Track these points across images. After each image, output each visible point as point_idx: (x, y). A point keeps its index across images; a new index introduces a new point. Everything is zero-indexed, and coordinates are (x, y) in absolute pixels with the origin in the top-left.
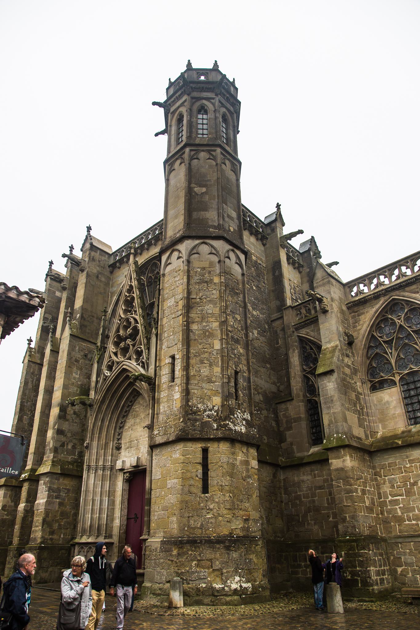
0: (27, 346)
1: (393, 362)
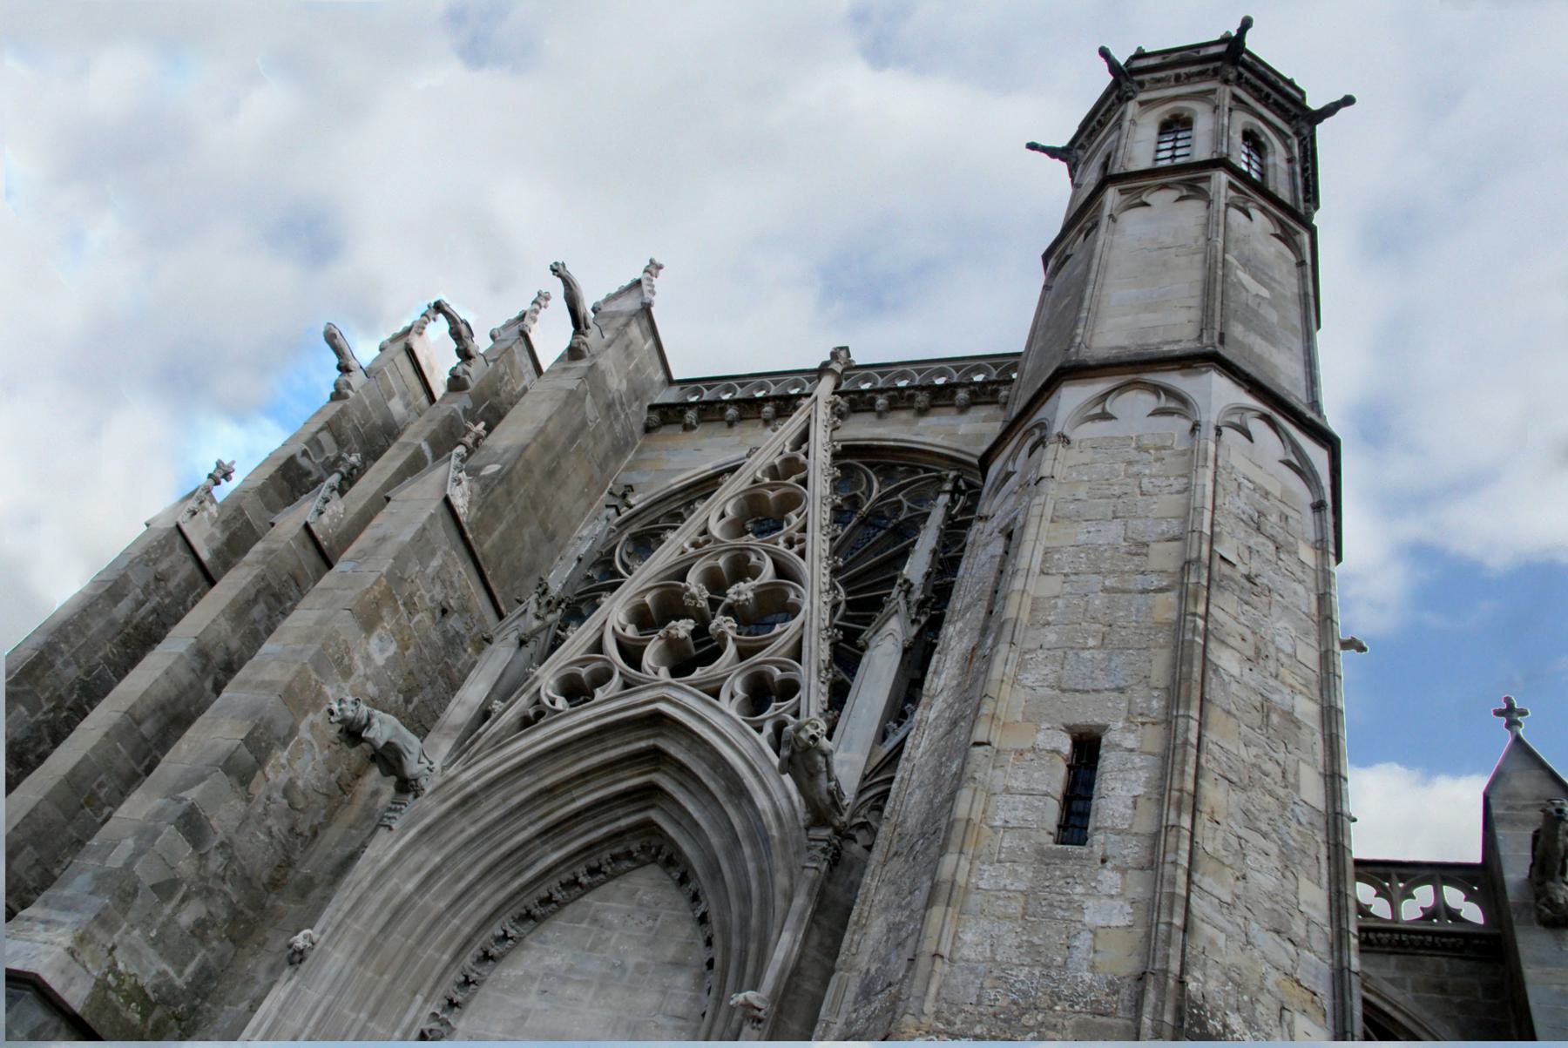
0: (203, 479)
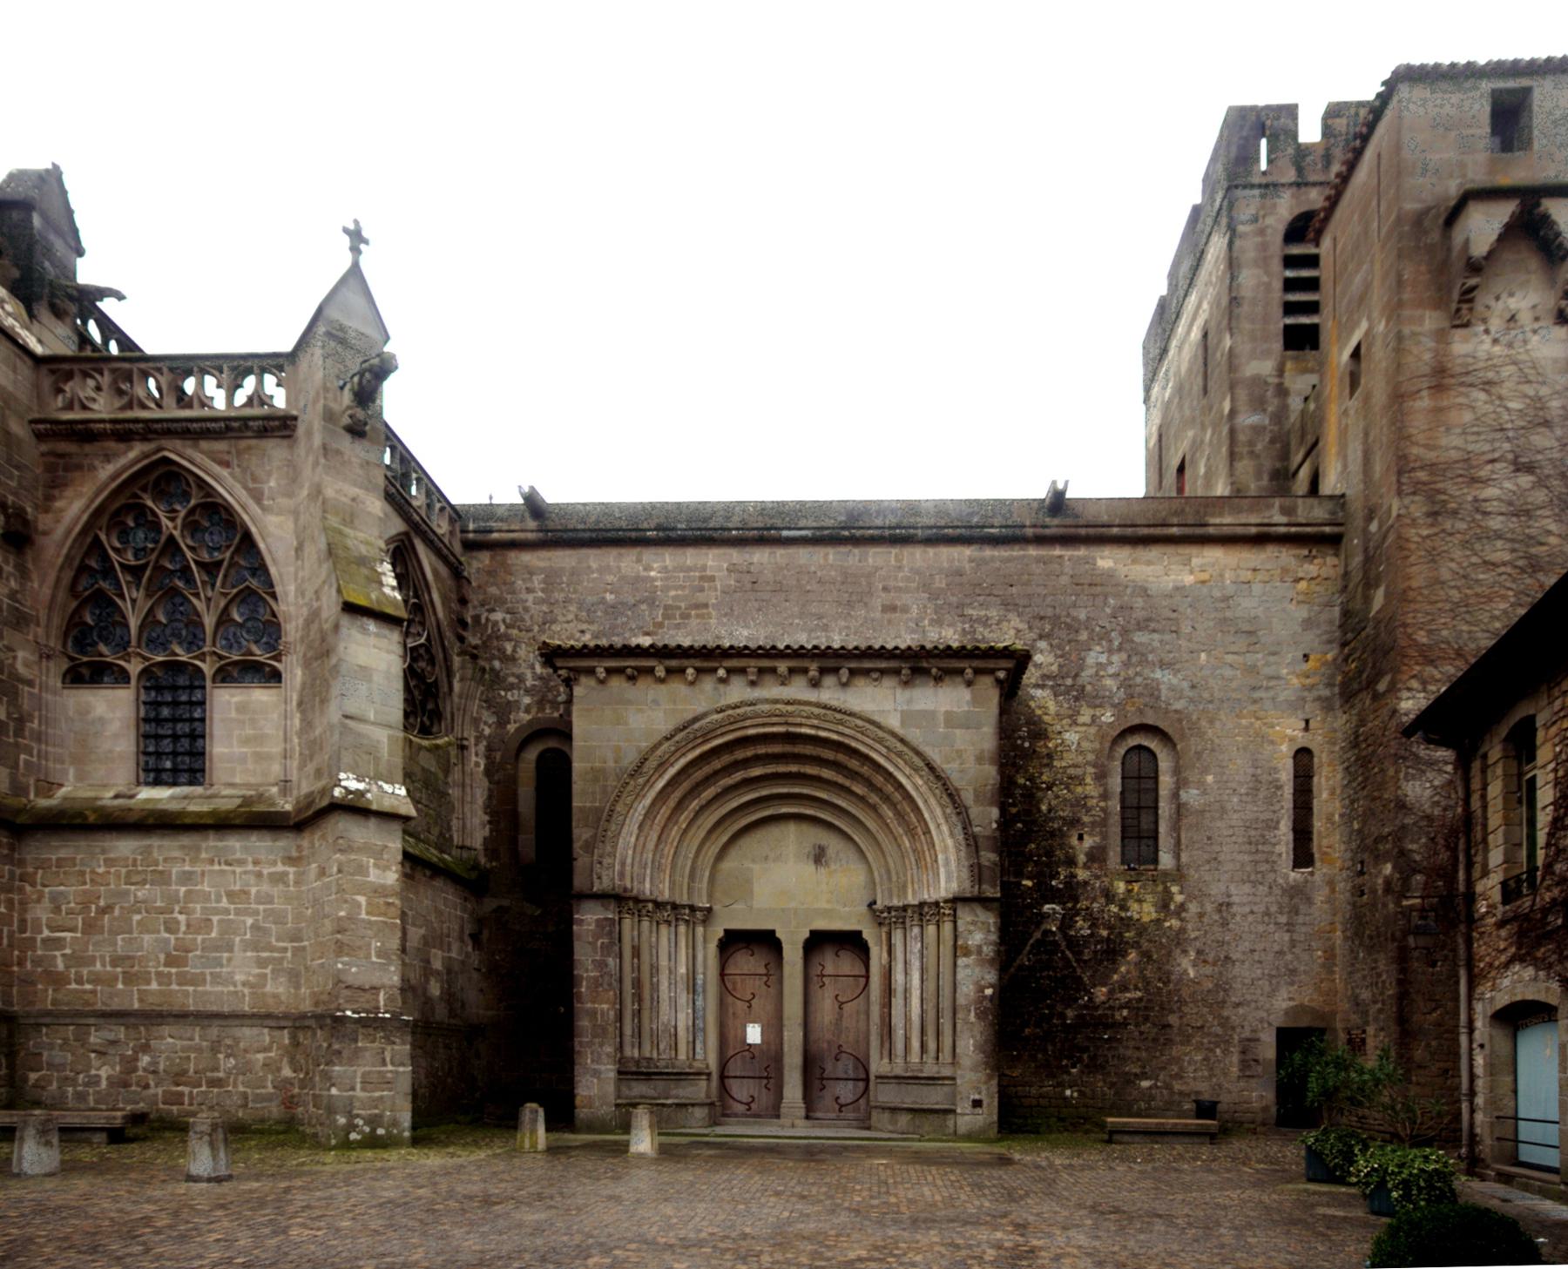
1: (134, 623)
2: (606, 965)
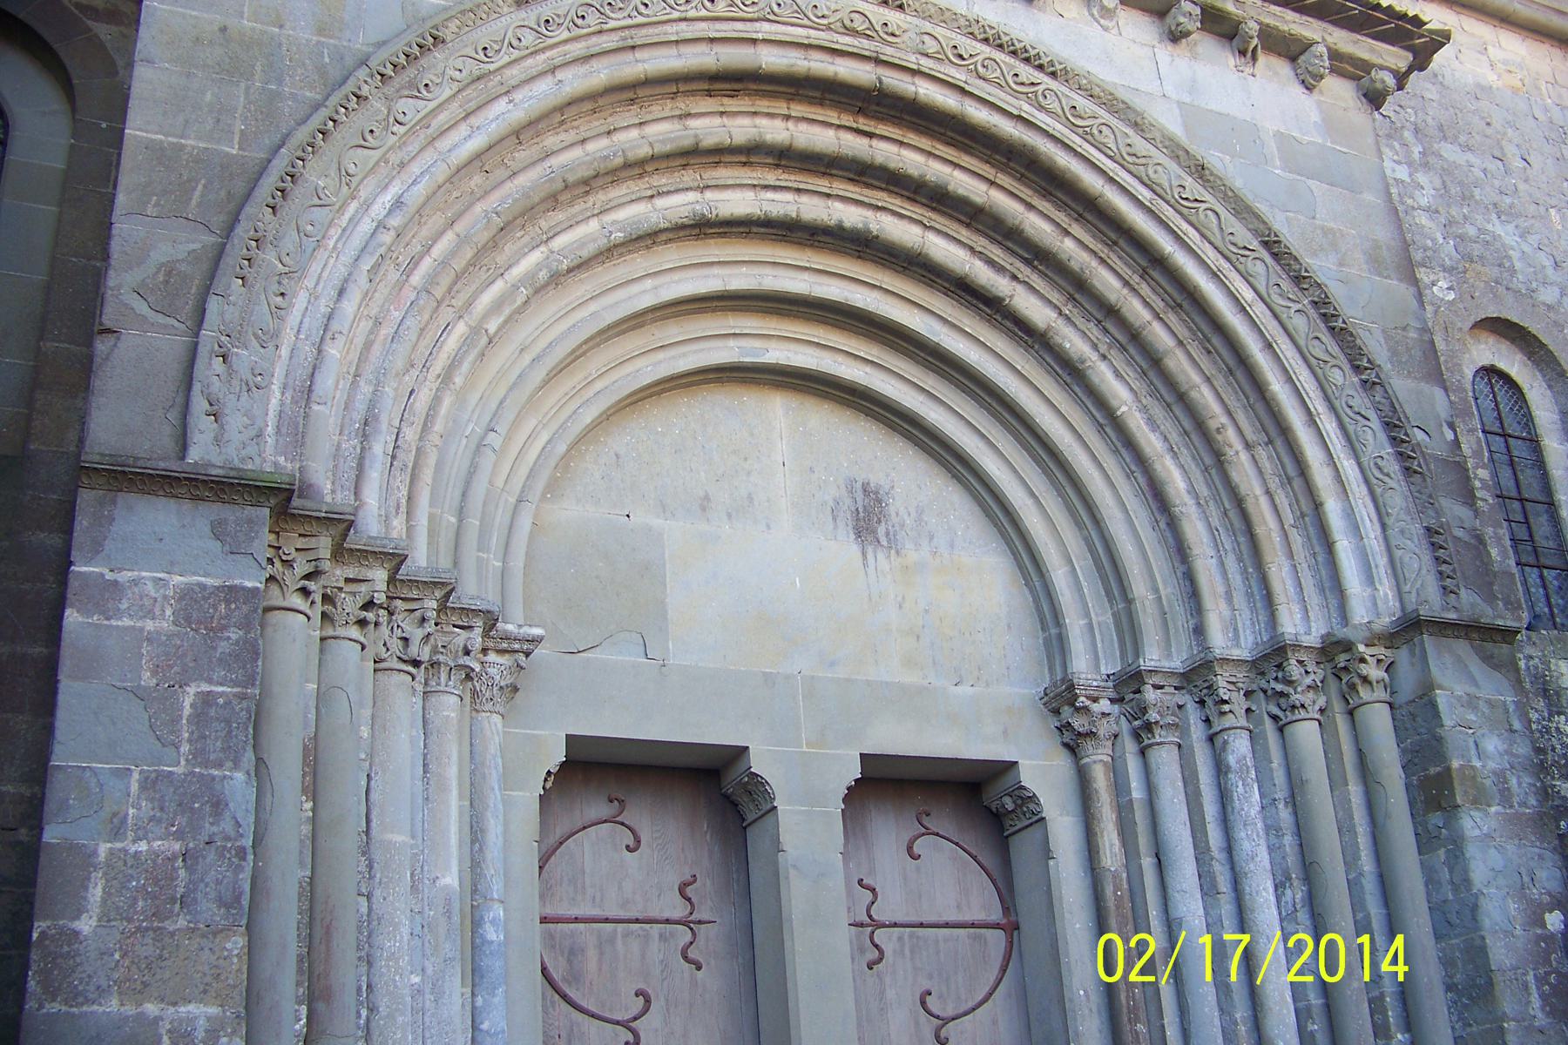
2: (219, 806)
